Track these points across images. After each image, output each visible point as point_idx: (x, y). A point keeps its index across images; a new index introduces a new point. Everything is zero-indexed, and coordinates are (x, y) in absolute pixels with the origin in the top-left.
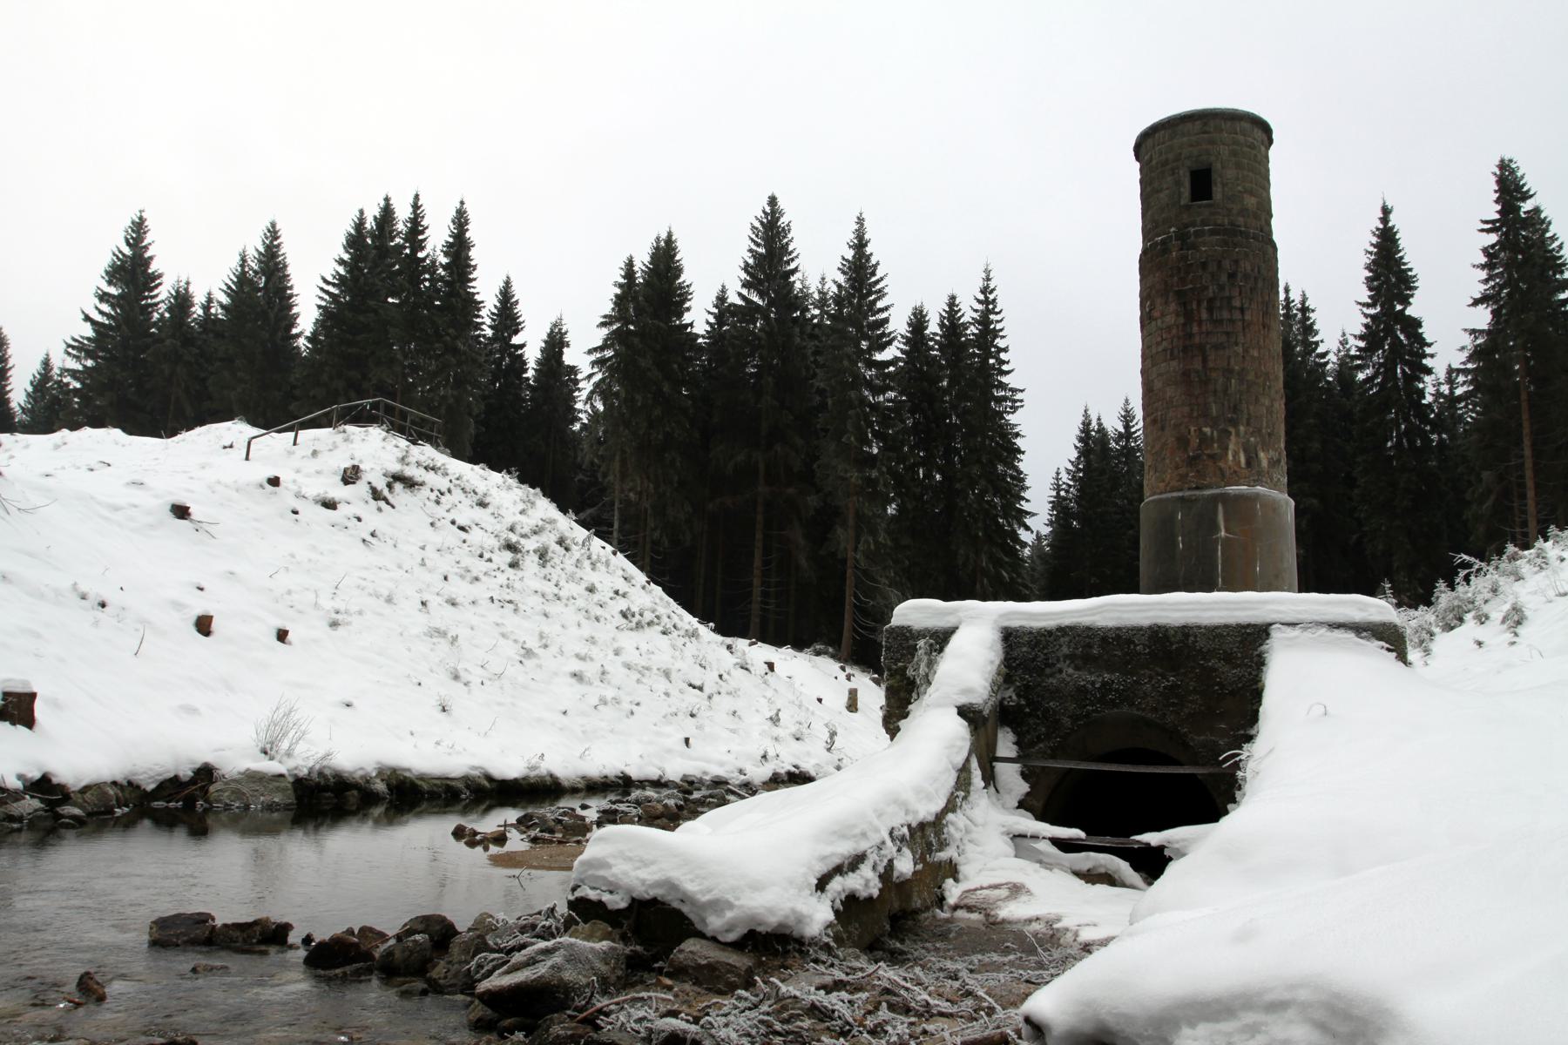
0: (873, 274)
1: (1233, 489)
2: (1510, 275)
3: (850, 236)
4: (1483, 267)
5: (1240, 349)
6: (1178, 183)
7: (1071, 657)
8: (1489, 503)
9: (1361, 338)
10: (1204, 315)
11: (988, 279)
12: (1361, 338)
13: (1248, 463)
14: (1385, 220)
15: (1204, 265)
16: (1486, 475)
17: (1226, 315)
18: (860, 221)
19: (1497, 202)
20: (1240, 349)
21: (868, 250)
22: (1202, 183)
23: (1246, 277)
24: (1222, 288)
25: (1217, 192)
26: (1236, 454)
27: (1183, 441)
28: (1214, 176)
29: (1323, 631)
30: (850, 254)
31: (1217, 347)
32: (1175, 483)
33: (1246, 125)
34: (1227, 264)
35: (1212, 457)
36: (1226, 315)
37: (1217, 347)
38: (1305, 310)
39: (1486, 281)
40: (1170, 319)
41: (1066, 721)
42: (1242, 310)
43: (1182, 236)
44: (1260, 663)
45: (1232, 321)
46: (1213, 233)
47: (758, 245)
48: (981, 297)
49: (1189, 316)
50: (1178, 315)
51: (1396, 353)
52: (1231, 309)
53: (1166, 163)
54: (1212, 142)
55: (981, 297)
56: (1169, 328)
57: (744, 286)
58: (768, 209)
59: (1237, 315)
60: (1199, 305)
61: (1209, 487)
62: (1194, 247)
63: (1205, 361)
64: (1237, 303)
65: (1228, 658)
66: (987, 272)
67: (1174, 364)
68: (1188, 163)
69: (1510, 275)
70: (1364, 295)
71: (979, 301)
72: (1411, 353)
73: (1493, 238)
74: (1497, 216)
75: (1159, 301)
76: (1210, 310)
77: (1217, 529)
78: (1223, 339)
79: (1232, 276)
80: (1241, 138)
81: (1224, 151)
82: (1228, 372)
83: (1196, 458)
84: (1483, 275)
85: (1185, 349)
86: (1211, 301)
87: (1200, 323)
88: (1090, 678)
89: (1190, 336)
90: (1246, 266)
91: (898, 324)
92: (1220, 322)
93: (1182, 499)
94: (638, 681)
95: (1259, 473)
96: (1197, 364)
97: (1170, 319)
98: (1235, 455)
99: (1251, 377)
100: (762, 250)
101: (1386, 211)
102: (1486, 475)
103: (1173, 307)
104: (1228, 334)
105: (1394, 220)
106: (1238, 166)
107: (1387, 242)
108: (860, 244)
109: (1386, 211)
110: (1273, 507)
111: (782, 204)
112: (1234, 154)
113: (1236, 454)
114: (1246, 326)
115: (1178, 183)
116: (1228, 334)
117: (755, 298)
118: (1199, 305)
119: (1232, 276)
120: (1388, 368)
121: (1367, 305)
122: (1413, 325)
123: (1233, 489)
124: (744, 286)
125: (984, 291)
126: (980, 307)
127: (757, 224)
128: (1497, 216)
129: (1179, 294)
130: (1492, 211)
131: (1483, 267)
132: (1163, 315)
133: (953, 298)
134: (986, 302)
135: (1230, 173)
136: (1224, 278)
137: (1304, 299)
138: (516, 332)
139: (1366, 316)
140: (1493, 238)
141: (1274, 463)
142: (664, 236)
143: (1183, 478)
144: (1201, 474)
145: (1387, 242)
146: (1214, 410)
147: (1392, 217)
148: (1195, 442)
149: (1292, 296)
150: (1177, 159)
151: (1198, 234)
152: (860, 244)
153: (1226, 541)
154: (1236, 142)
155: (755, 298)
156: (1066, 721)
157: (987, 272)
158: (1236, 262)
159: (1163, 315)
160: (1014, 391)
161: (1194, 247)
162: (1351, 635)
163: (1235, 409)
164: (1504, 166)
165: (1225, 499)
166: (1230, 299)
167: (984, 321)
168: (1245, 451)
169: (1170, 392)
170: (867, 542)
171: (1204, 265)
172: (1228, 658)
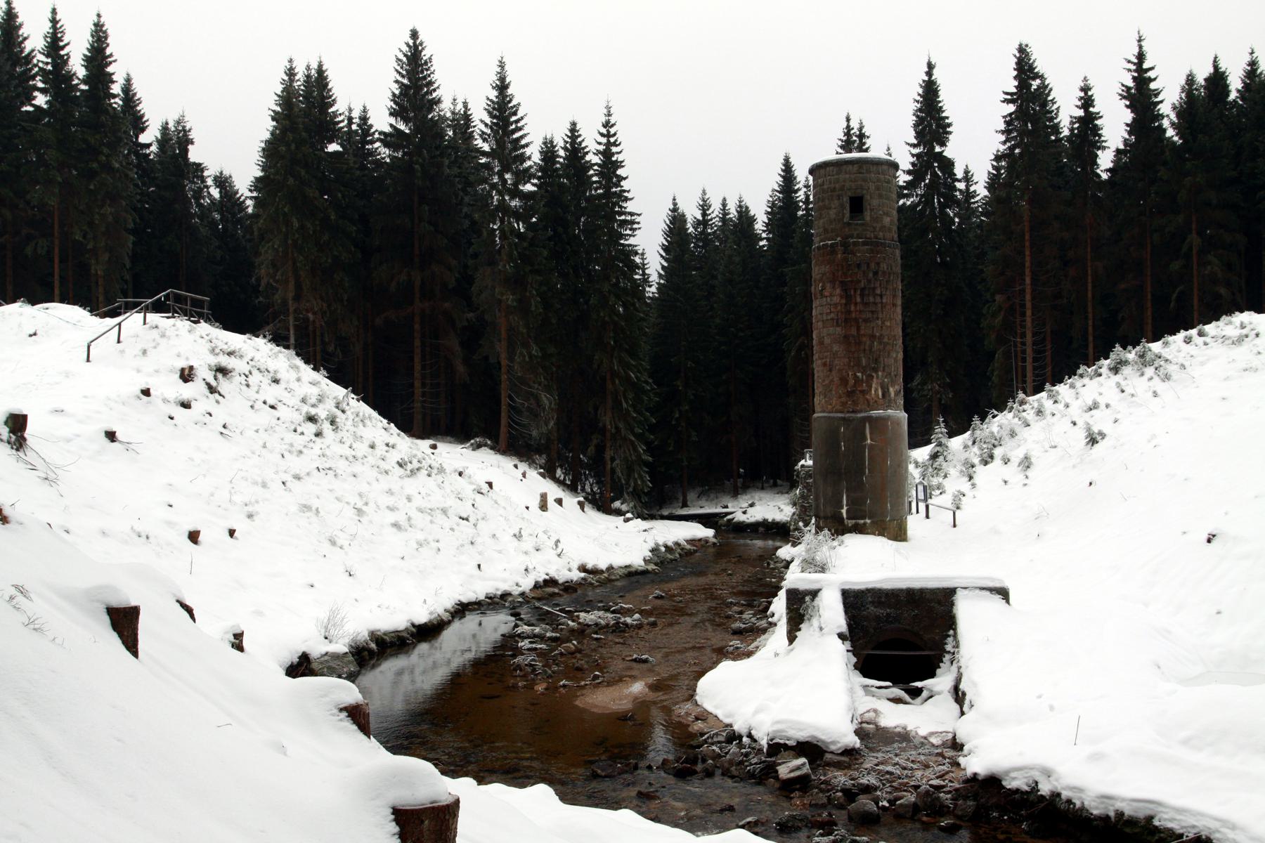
0: (515, 114)
1: (874, 413)
2: (1022, 140)
3: (493, 78)
4: (1003, 132)
5: (879, 322)
7: (872, 602)
8: (1000, 318)
9: (909, 172)
10: (859, 300)
11: (609, 115)
12: (909, 172)
13: (884, 395)
14: (929, 74)
15: (859, 266)
16: (998, 297)
17: (871, 299)
18: (502, 65)
19: (1015, 78)
20: (879, 322)
21: (510, 91)
22: (857, 205)
23: (884, 272)
24: (869, 281)
25: (867, 216)
26: (876, 390)
27: (844, 381)
28: (865, 204)
29: (977, 591)
30: (493, 94)
31: (866, 321)
32: (838, 407)
33: (885, 167)
34: (873, 265)
35: (863, 392)
36: (871, 299)
37: (866, 321)
39: (1004, 143)
40: (836, 299)
41: (872, 630)
42: (881, 296)
43: (845, 245)
44: (952, 604)
45: (875, 304)
46: (864, 244)
47: (403, 76)
48: (604, 131)
49: (848, 298)
50: (841, 297)
51: (933, 187)
52: (875, 295)
53: (834, 190)
54: (865, 180)
55: (604, 131)
56: (836, 305)
57: (391, 114)
58: (411, 42)
59: (878, 300)
60: (855, 290)
61: (861, 411)
62: (853, 253)
63: (858, 329)
64: (878, 292)
65: (939, 603)
66: (608, 108)
67: (839, 329)
68: (850, 194)
69: (1022, 140)
70: (911, 137)
71: (602, 135)
72: (945, 184)
73: (1011, 108)
74: (1015, 90)
75: (828, 285)
76: (862, 296)
77: (865, 439)
78: (869, 315)
79: (876, 273)
80: (882, 177)
81: (872, 187)
82: (872, 337)
83: (853, 392)
84: (1003, 138)
85: (846, 321)
86: (863, 290)
87: (856, 304)
88: (881, 612)
89: (849, 312)
90: (884, 266)
91: (534, 154)
92: (866, 304)
93: (844, 419)
94: (431, 522)
95: (890, 401)
96: (854, 331)
97: (836, 299)
98: (876, 391)
99: (886, 340)
100: (405, 81)
101: (931, 66)
102: (998, 297)
103: (838, 291)
104: (872, 312)
105: (937, 74)
106: (880, 196)
107: (930, 91)
108: (502, 87)
109: (931, 66)
110: (897, 422)
111: (422, 37)
112: (878, 188)
113: (876, 390)
114: (883, 306)
115: (842, 206)
116: (872, 312)
117: (402, 126)
118: (855, 290)
119: (876, 273)
120: (927, 199)
121: (914, 146)
122: (948, 165)
123: (874, 413)
124: (391, 114)
125: (607, 125)
126: (604, 140)
127: (401, 56)
128: (1015, 90)
130: (1012, 86)
131: (1003, 132)
132: (831, 295)
133: (574, 124)
134: (608, 135)
135: (875, 202)
136: (871, 275)
137: (861, 129)
138: (143, 130)
139: (913, 155)
140: (1011, 108)
141: (897, 393)
142: (314, 66)
143: (844, 404)
144: (855, 403)
145: (930, 91)
146: (864, 362)
147: (935, 71)
148: (852, 382)
149: (852, 124)
150: (842, 188)
151: (855, 244)
152: (502, 87)
153: (871, 447)
154: (879, 180)
155: (402, 126)
156: (872, 630)
157: (608, 108)
158: (878, 264)
159: (831, 295)
160: (632, 214)
161: (853, 253)
162: (988, 593)
163: (876, 361)
164: (1022, 50)
165: (870, 419)
166: (874, 289)
167: (607, 154)
168: (882, 388)
169: (836, 348)
170: (521, 353)
171: (859, 266)
172: (939, 603)
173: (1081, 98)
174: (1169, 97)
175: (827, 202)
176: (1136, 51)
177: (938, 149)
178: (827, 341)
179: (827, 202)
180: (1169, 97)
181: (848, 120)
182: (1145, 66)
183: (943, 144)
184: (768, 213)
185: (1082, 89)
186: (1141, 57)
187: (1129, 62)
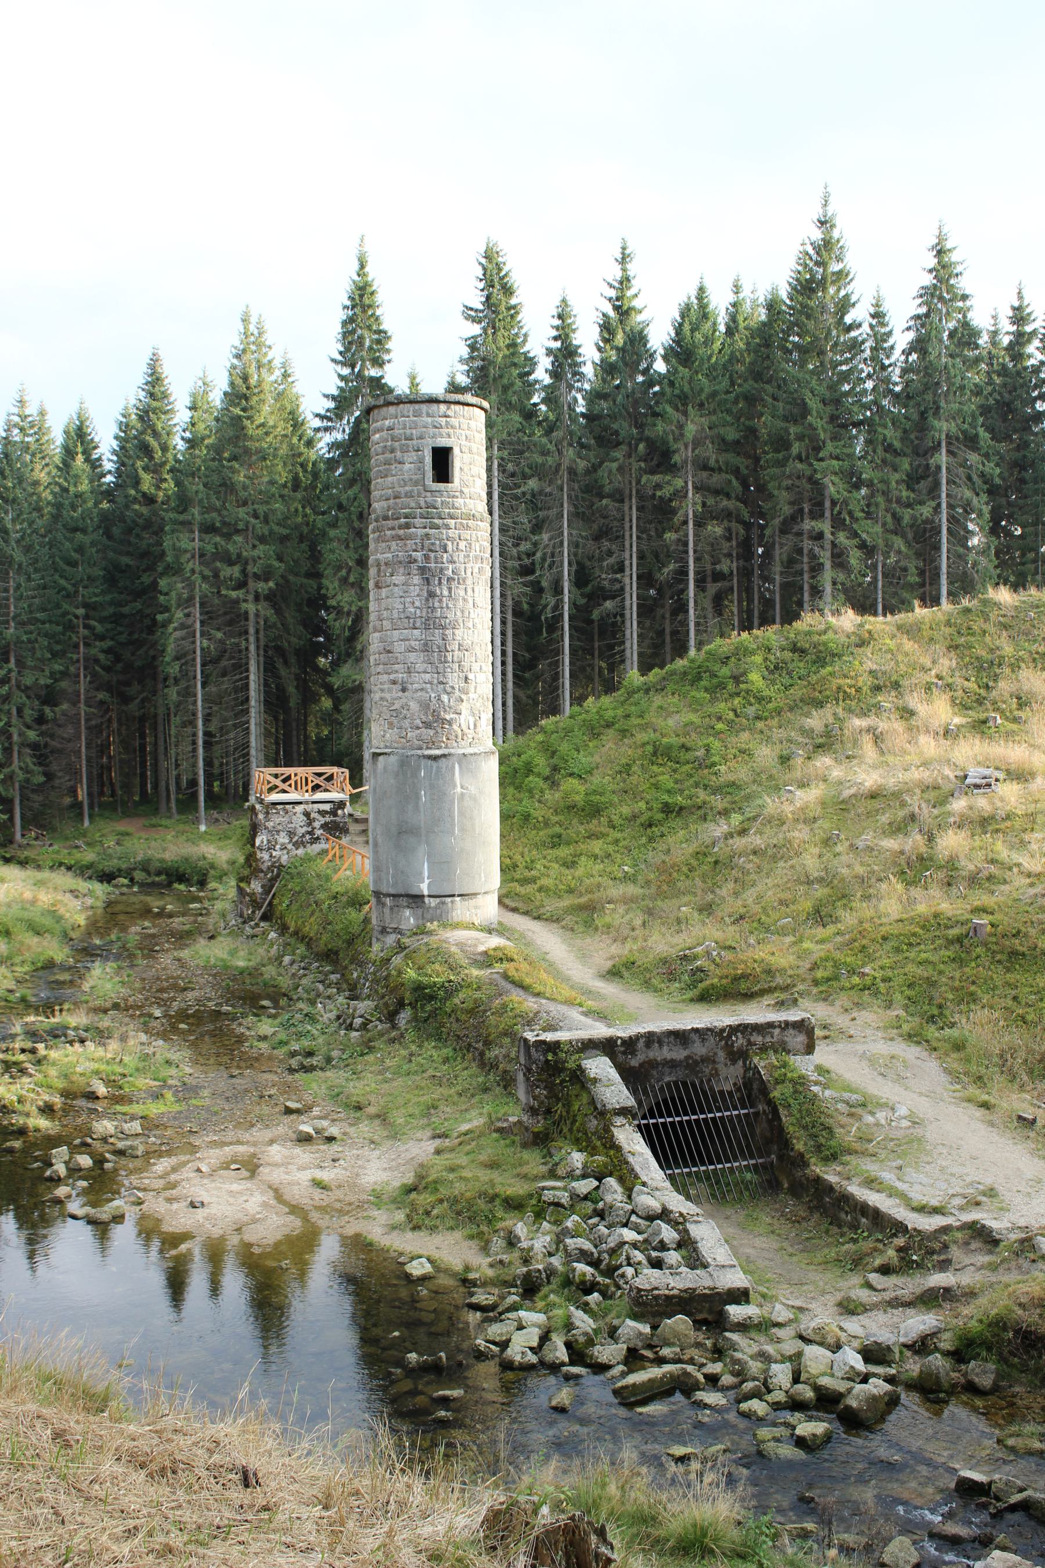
6: (421, 461)
10: (446, 593)
38: (259, 345)
64: (469, 582)
73: (476, 329)
74: (481, 307)
76: (450, 589)
77: (455, 786)
103: (416, 580)
107: (361, 300)
128: (481, 307)
129: (422, 570)
130: (477, 301)
140: (476, 329)
145: (361, 300)
168: (474, 715)
173: (557, 328)
174: (659, 336)
175: (398, 454)
176: (619, 275)
177: (373, 372)
178: (399, 647)
179: (398, 454)
180: (659, 336)
181: (245, 321)
182: (629, 293)
183: (378, 363)
184: (116, 438)
185: (560, 317)
186: (625, 282)
187: (611, 286)
